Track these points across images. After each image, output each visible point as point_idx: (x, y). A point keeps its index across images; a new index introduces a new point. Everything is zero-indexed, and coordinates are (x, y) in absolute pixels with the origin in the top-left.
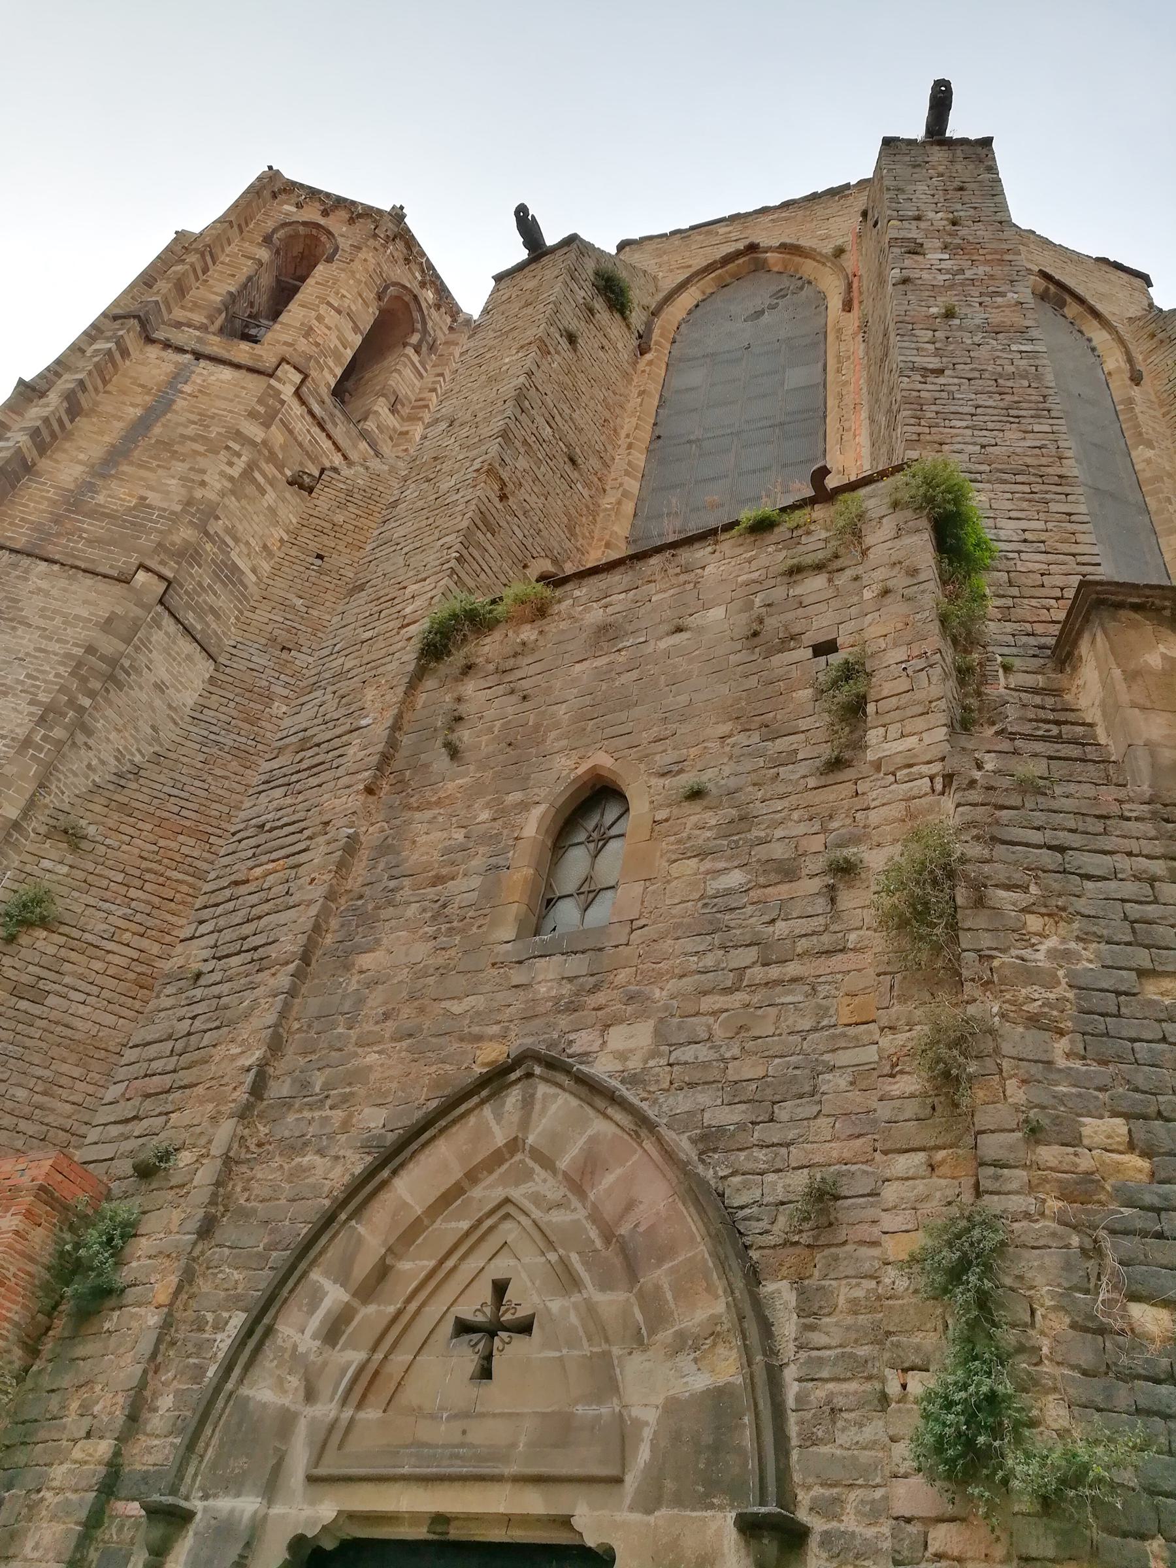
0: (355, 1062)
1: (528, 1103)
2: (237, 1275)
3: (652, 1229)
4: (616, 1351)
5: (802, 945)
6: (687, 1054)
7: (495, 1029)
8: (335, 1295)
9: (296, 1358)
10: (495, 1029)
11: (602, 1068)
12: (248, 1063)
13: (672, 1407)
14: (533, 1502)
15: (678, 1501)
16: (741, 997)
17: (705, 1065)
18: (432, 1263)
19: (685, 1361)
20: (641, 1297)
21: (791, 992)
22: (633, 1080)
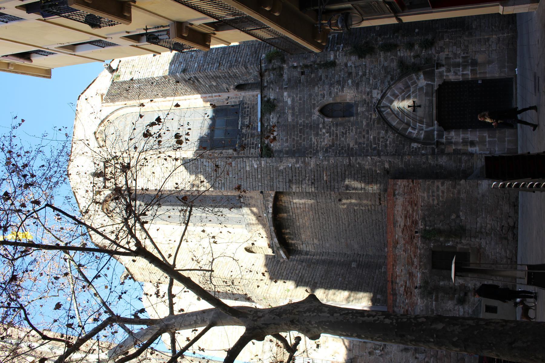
0: (372, 141)
1: (383, 107)
2: (406, 148)
3: (404, 85)
4: (418, 88)
5: (364, 70)
6: (379, 84)
7: (370, 116)
8: (410, 130)
9: (418, 132)
10: (370, 116)
11: (379, 97)
12: (370, 159)
13: (425, 79)
14: (434, 95)
15: (434, 76)
16: (371, 78)
17: (381, 81)
18: (406, 117)
19: (420, 78)
20: (412, 85)
21: (371, 71)
22: (382, 91)
